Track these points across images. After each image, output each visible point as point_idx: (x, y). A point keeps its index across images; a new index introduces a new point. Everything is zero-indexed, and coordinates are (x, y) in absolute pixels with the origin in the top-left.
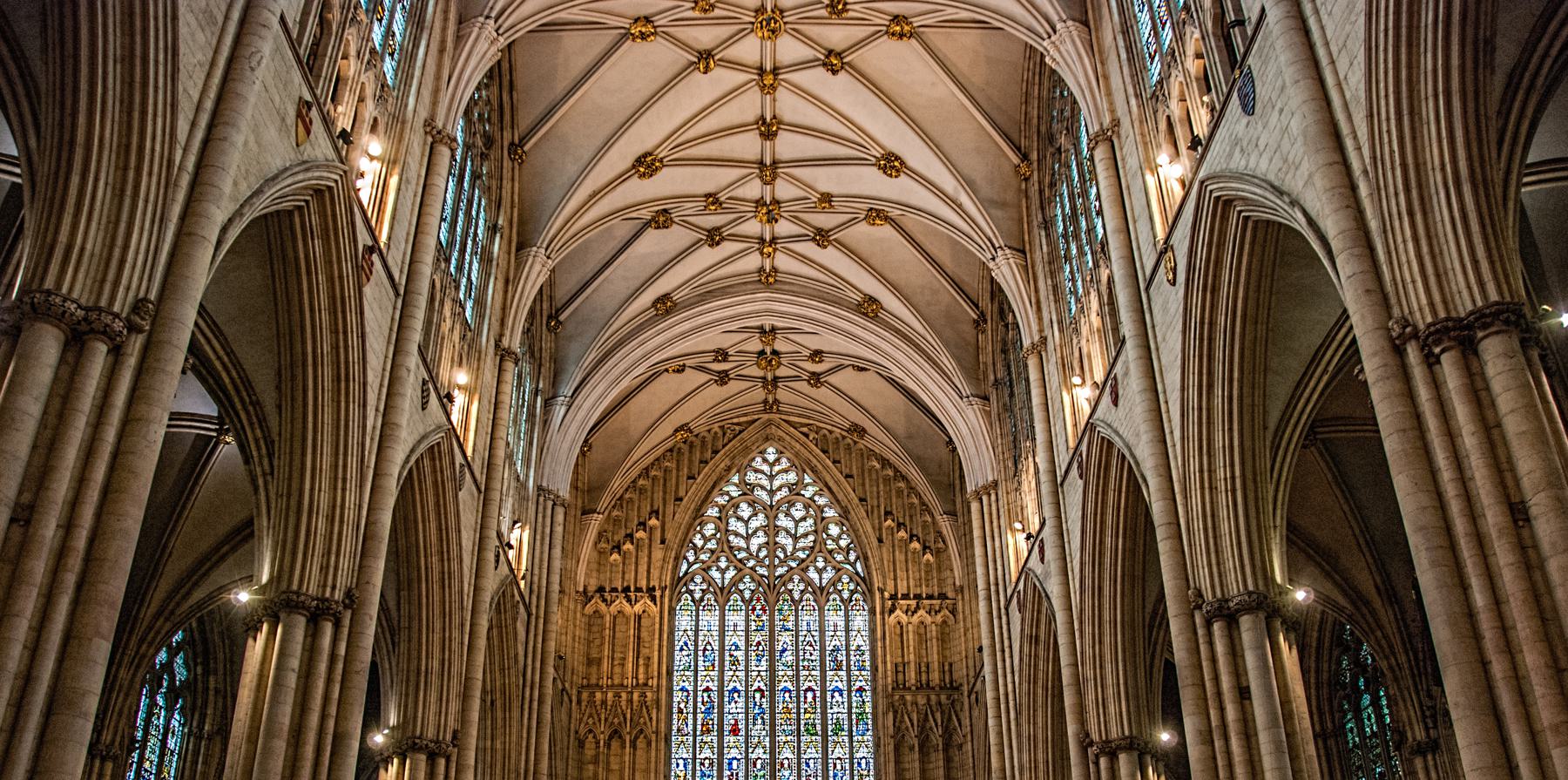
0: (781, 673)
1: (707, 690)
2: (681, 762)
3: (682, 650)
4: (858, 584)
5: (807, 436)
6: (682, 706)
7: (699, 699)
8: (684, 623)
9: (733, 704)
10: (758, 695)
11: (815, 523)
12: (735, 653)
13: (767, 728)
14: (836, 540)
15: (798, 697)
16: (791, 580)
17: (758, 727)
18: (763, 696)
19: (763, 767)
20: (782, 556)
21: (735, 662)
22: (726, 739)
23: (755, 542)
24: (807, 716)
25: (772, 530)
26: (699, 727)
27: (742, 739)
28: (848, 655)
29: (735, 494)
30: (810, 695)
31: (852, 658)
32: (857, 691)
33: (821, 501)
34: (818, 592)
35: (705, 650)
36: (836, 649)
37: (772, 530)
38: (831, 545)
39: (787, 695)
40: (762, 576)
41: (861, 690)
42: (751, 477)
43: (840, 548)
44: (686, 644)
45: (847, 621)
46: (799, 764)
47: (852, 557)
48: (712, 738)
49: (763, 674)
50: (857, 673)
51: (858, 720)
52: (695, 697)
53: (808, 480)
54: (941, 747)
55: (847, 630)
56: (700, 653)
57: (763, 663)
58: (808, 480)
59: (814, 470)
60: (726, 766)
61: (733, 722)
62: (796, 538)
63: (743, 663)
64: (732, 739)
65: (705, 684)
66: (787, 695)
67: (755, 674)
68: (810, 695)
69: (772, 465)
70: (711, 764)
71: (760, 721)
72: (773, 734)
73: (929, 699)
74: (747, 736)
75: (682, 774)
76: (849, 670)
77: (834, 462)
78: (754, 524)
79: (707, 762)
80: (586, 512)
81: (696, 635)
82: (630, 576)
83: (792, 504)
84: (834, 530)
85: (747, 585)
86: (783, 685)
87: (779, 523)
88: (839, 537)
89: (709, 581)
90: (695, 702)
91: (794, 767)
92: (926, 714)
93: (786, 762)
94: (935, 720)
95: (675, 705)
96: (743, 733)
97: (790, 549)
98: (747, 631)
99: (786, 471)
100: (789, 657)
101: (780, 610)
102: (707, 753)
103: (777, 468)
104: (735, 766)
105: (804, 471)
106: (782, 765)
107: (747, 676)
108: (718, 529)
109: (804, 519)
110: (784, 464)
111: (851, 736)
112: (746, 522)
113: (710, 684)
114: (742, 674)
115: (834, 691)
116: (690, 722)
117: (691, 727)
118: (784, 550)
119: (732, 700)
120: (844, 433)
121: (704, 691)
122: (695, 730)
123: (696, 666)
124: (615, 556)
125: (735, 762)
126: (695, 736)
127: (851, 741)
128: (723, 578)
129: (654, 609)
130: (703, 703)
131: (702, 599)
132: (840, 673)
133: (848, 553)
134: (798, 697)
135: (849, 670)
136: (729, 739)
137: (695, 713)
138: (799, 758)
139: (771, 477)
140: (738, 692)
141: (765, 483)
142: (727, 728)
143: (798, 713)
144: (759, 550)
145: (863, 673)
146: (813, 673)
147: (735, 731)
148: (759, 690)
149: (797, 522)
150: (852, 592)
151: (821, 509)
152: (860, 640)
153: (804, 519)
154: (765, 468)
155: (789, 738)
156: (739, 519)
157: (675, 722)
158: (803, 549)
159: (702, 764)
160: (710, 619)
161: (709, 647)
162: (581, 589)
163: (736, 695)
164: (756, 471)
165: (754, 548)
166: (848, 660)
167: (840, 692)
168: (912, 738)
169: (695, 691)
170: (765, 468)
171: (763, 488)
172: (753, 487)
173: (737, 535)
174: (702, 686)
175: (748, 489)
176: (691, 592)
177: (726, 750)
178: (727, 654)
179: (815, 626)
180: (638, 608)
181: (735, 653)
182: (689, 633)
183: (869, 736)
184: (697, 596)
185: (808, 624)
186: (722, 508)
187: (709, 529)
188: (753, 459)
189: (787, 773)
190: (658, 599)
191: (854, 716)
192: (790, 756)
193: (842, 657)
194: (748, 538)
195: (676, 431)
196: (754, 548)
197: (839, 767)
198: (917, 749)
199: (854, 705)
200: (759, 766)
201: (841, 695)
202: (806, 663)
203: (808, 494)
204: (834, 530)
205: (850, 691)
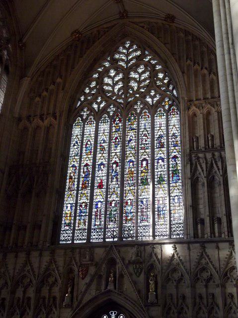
0: (128, 153)
1: (87, 165)
2: (69, 205)
3: (74, 145)
4: (173, 101)
5: (143, 27)
6: (72, 175)
7: (82, 171)
8: (77, 132)
9: (100, 172)
10: (114, 166)
11: (150, 74)
12: (103, 144)
13: (119, 183)
14: (162, 80)
15: (138, 164)
16: (136, 103)
17: (114, 183)
18: (117, 166)
19: (116, 205)
20: (131, 92)
21: (103, 149)
22: (95, 191)
23: (117, 87)
24: (143, 174)
25: (126, 80)
26: (81, 185)
27: (104, 190)
28: (168, 139)
29: (107, 66)
30: (144, 163)
31: (170, 140)
32: (173, 158)
33: (153, 62)
34: (150, 107)
35: (87, 144)
36: (161, 137)
37: (126, 80)
38: (158, 83)
39: (131, 164)
40: (121, 103)
41: (175, 157)
42: (117, 56)
43: (164, 83)
44: (77, 142)
45: (168, 121)
46: (137, 202)
47: (171, 88)
48: (87, 191)
49: (118, 154)
50: (173, 148)
51: (173, 174)
52: (80, 169)
53: (147, 53)
54: (222, 182)
55: (167, 125)
56: (84, 146)
57: (119, 148)
58: (147, 53)
59: (149, 47)
60: (94, 206)
61: (99, 181)
62: (139, 82)
63: (107, 149)
64: (99, 190)
65: (86, 162)
66: (131, 164)
67: (113, 154)
68: (144, 163)
69: (128, 49)
70: (86, 206)
71: (115, 180)
72: (122, 186)
73: (213, 155)
74: (107, 188)
75: (69, 212)
76: (168, 147)
77: (158, 38)
78: (117, 79)
79: (84, 204)
80: (22, 77)
81: (83, 138)
82: (45, 109)
83: (137, 66)
84: (161, 76)
85: (112, 110)
86: (129, 158)
87: (131, 76)
88: (164, 78)
89: (91, 110)
90: (79, 172)
91: (134, 204)
92: (212, 164)
93: (129, 201)
94: (218, 167)
95: (68, 175)
96: (105, 187)
97: (136, 88)
98: (110, 132)
99: (135, 51)
100: (133, 144)
101: (129, 120)
102: (84, 200)
103: (131, 50)
104: (99, 206)
105: (145, 50)
106: (127, 203)
107: (109, 156)
108: (97, 84)
109: (144, 72)
110: (135, 47)
111: (169, 184)
112: (113, 78)
113: (88, 162)
114: (106, 155)
115: (159, 159)
116: (76, 183)
117: (76, 186)
118: (132, 88)
119: (100, 169)
120: (164, 22)
121: (85, 166)
122: (78, 187)
123: (81, 153)
124: (37, 99)
125: (99, 204)
126: (78, 190)
127: (169, 187)
128: (99, 107)
129: (56, 123)
130: (84, 172)
131: (87, 119)
132: (162, 149)
133: (168, 87)
134: (138, 164)
135: (168, 147)
136: (97, 191)
137: (79, 179)
138: (137, 198)
139: (127, 55)
140: (104, 165)
141: (124, 58)
142: (96, 185)
143: (138, 173)
144: (119, 90)
145: (176, 148)
146: (147, 151)
147: (100, 186)
148: (116, 163)
149: (140, 75)
150: (170, 106)
151: (154, 66)
152: (175, 130)
153: (144, 72)
154: (124, 51)
155: (131, 188)
156: (109, 77)
157: (67, 184)
158: (143, 87)
159: (81, 206)
160: (90, 129)
161: (89, 143)
162: (17, 116)
163: (102, 167)
164: (120, 53)
165: (116, 91)
166: (168, 142)
167: (163, 160)
168: (203, 179)
169: (80, 166)
170: (124, 51)
171: (123, 60)
172: (118, 60)
173: (108, 85)
174: (84, 163)
175: (114, 62)
176: (82, 116)
177: (95, 197)
178: (99, 145)
179: (148, 126)
180: (46, 122)
181: (103, 144)
182: (79, 137)
183: (179, 183)
184: (84, 117)
185: (145, 125)
186: (99, 73)
187: (93, 84)
188: (118, 48)
189: (129, 208)
190: (58, 117)
191: (171, 172)
192: (132, 198)
193: (164, 140)
194: (113, 87)
195: (72, 33)
196: (116, 91)
197: (161, 202)
198: (206, 184)
199: (171, 166)
200: (113, 205)
201: (163, 161)
202: (143, 146)
203: (147, 60)
204: (161, 76)
205: (168, 159)
